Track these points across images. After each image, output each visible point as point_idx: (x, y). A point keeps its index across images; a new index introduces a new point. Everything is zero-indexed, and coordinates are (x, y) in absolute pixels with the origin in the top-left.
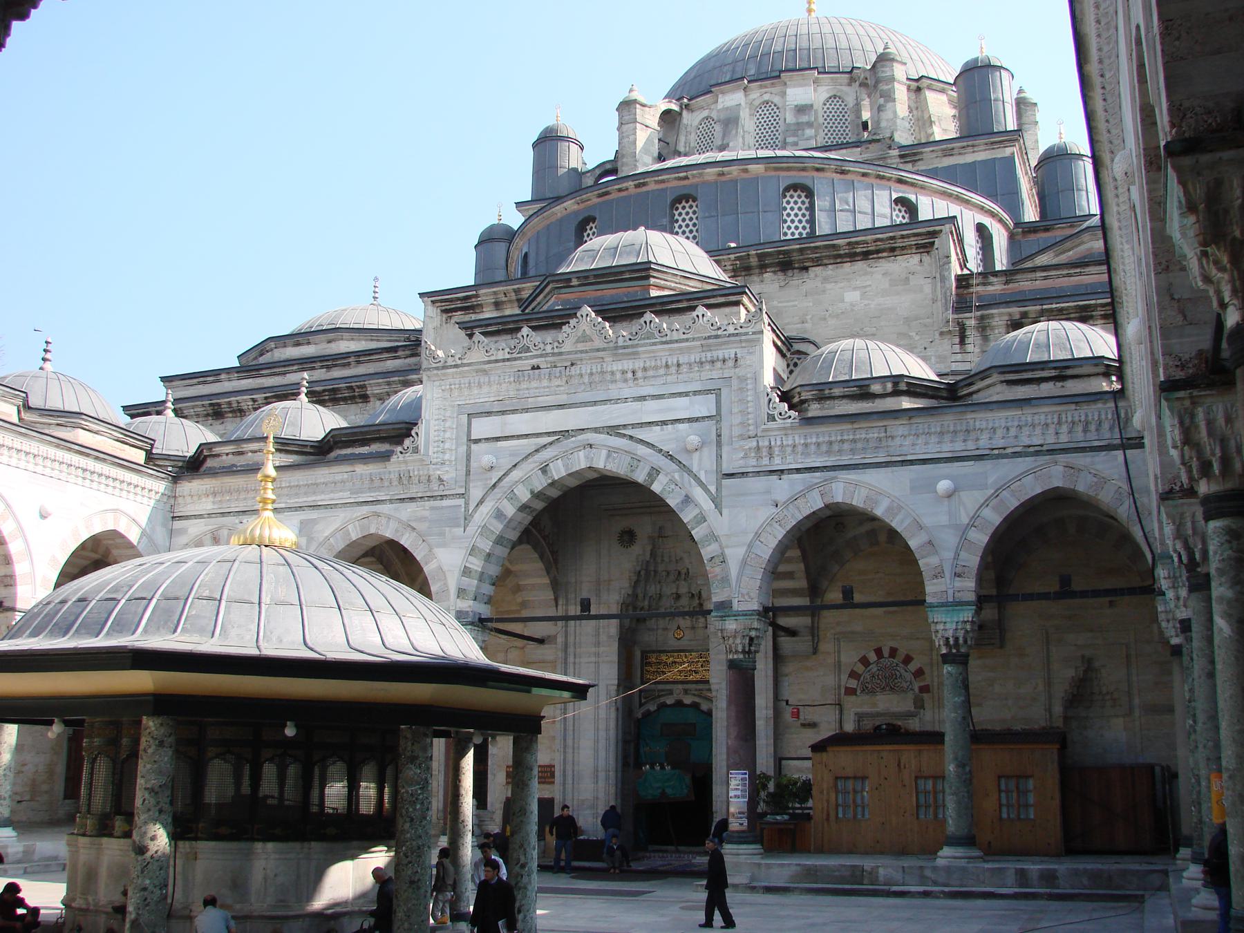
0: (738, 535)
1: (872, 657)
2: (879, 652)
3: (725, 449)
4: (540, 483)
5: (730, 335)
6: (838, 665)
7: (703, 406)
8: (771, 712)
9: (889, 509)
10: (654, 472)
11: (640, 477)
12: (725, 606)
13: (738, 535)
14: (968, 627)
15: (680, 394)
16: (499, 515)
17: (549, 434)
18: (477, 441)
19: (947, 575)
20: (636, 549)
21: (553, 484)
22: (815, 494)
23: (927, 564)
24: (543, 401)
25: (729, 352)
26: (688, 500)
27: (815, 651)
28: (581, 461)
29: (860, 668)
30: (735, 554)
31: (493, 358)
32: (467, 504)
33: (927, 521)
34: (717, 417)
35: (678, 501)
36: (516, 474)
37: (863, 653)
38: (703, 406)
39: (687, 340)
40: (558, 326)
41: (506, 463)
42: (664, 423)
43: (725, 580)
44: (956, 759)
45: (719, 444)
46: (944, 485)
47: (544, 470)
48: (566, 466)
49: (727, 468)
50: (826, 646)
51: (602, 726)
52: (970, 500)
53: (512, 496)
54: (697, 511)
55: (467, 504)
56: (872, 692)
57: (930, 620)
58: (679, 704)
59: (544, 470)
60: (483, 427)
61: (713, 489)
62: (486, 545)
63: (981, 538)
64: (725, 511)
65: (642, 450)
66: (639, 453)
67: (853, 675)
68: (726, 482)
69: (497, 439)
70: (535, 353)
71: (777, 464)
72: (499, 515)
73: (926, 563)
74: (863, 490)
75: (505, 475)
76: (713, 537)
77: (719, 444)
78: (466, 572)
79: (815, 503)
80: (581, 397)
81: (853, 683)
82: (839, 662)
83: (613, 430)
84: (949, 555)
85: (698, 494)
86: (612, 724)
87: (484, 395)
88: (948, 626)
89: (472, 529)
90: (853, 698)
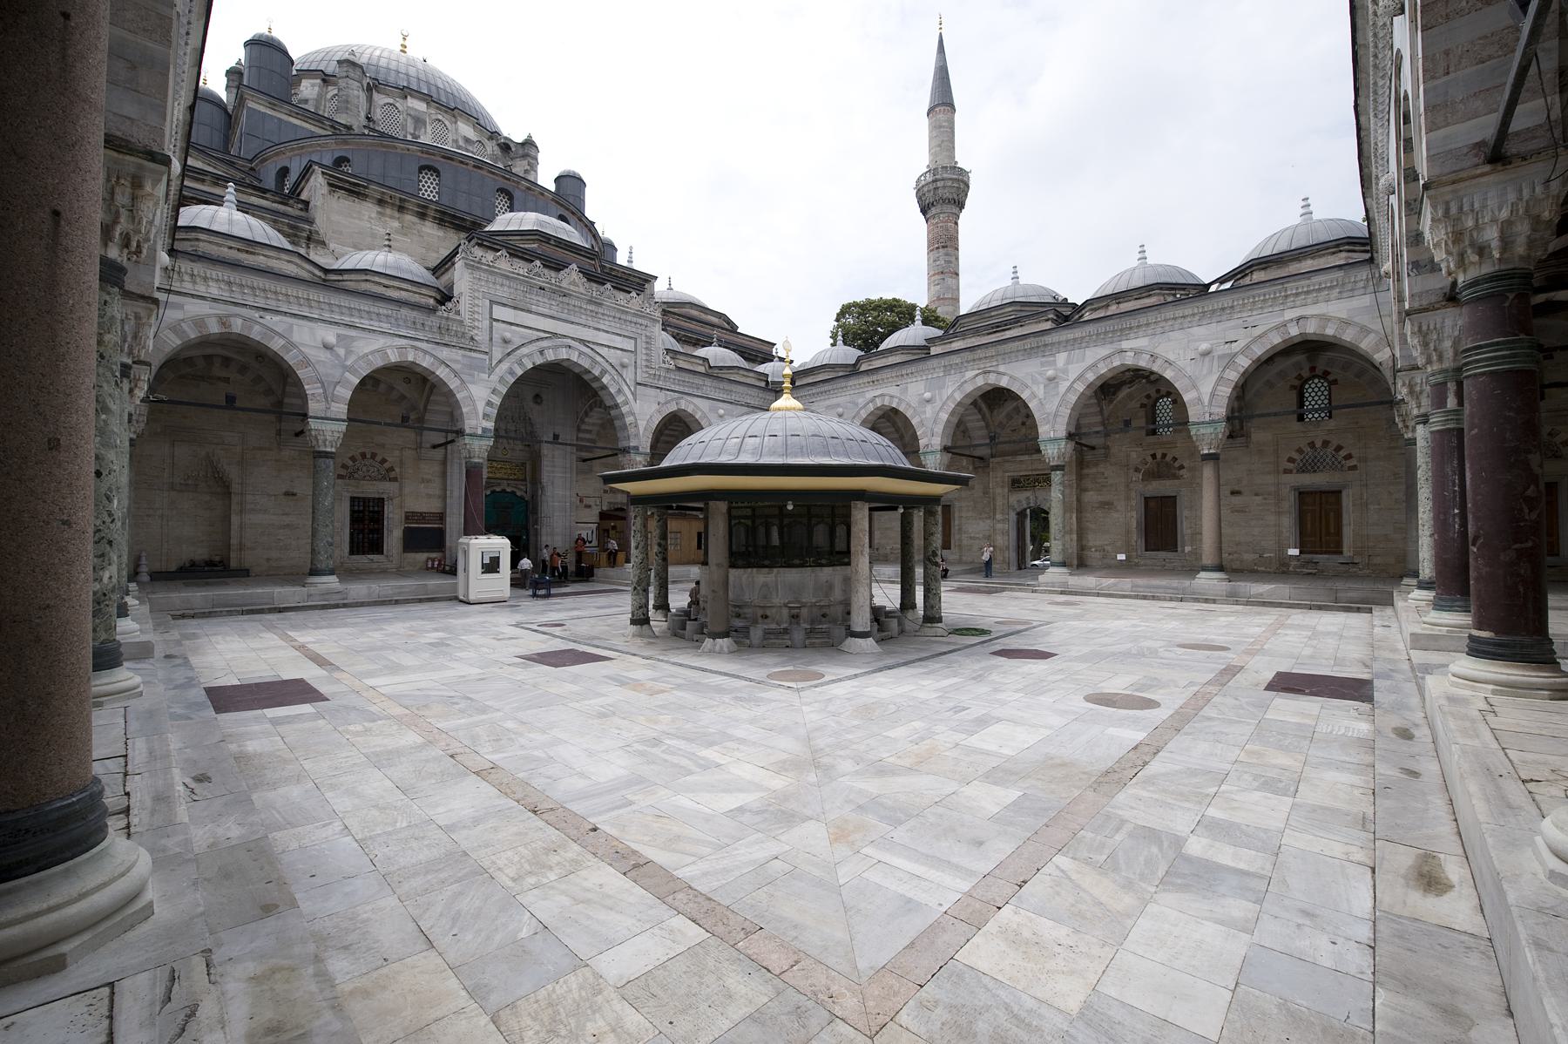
4: (539, 361)
7: (629, 345)
10: (604, 372)
12: (636, 448)
16: (511, 372)
24: (541, 310)
25: (644, 322)
26: (620, 391)
28: (563, 354)
30: (642, 424)
34: (634, 352)
36: (525, 350)
38: (629, 345)
40: (558, 270)
41: (517, 341)
43: (637, 435)
47: (541, 352)
53: (521, 364)
58: (504, 491)
59: (541, 352)
60: (499, 312)
65: (598, 359)
71: (661, 384)
78: (489, 404)
79: (673, 408)
80: (564, 316)
85: (625, 388)
87: (503, 292)
89: (495, 377)
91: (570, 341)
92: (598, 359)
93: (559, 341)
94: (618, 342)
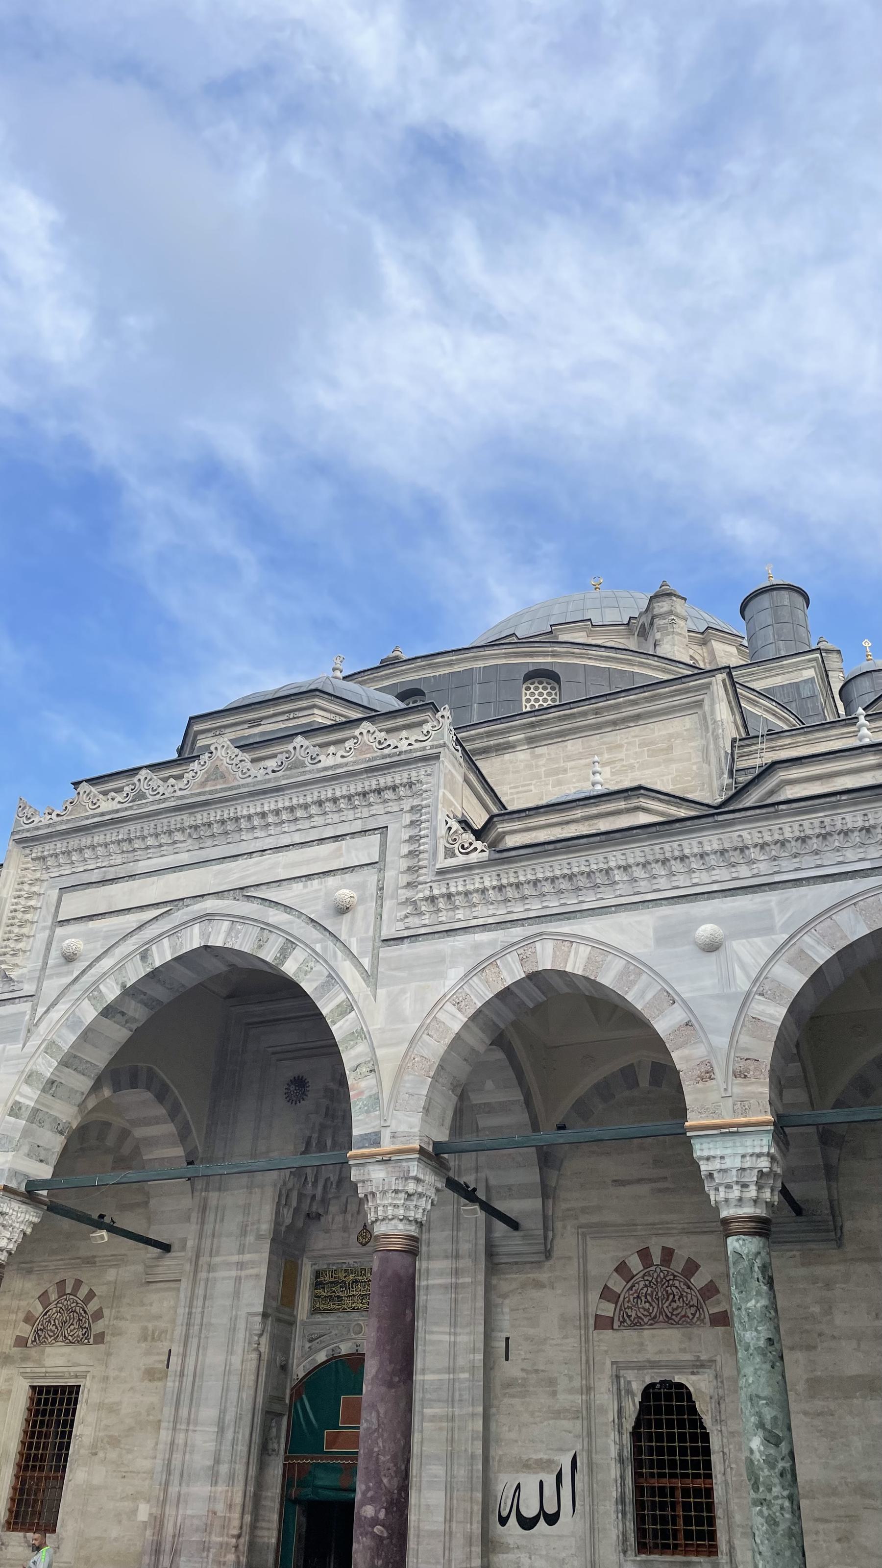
0: (399, 1024)
1: (635, 1264)
2: (644, 1255)
3: (388, 904)
4: (135, 973)
5: (400, 753)
6: (584, 1281)
7: (363, 850)
8: (480, 1357)
9: (623, 974)
11: (269, 955)
13: (399, 1024)
14: (764, 1164)
15: (336, 838)
17: (157, 905)
18: (62, 923)
19: (719, 1074)
20: (307, 1104)
21: (154, 975)
22: (512, 959)
23: (687, 1059)
26: (333, 979)
27: (548, 1254)
28: (193, 939)
29: (617, 1284)
30: (389, 1057)
31: (98, 811)
32: (34, 1010)
33: (685, 990)
35: (315, 985)
37: (621, 1254)
39: (346, 764)
42: (308, 877)
44: (761, 1425)
45: (380, 898)
46: (706, 930)
47: (144, 956)
48: (173, 948)
49: (386, 933)
50: (566, 1242)
51: (234, 1381)
52: (749, 953)
54: (342, 996)
55: (34, 1010)
56: (636, 1324)
57: (697, 1153)
61: (366, 962)
62: (47, 1067)
63: (775, 1013)
64: (381, 992)
65: (275, 917)
66: (271, 920)
67: (607, 1294)
68: (387, 952)
69: (91, 917)
70: (151, 799)
72: (71, 1021)
73: (682, 1058)
74: (582, 947)
75: (90, 966)
76: (360, 1034)
77: (380, 898)
79: (512, 972)
81: (608, 1309)
82: (585, 1271)
83: (242, 892)
84: (721, 1041)
85: (348, 971)
86: (250, 1379)
88: (728, 1163)
90: (608, 1335)
91: (210, 905)
92: (275, 917)
93: (180, 915)
94: (323, 856)
